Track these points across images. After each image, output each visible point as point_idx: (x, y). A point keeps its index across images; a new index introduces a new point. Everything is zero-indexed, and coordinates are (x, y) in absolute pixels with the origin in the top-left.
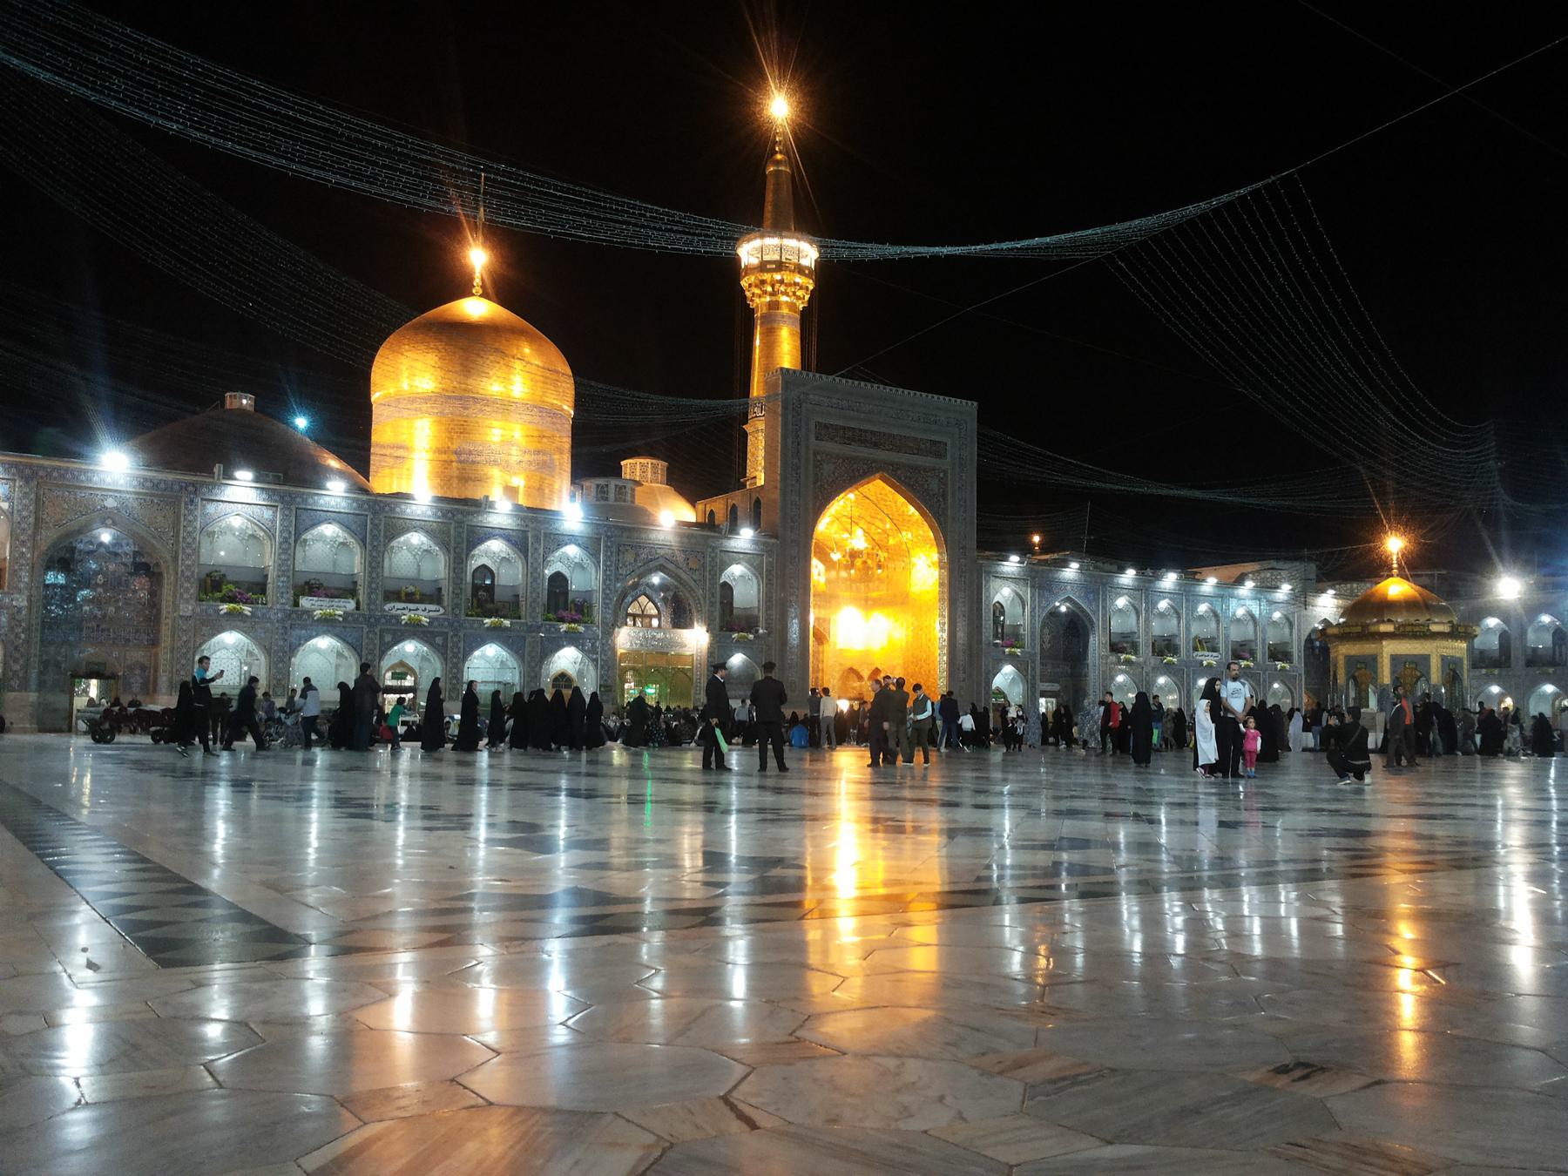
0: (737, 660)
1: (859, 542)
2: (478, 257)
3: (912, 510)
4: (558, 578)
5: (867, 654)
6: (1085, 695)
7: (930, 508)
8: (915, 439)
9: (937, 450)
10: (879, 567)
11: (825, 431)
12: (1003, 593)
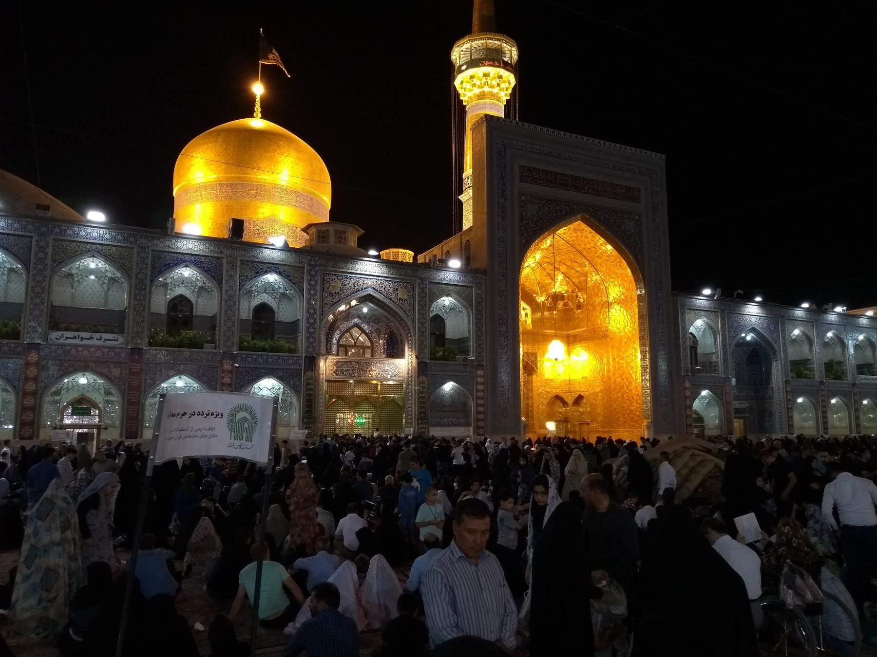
0: (448, 387)
1: (560, 286)
2: (258, 89)
3: (609, 247)
4: (263, 310)
5: (570, 382)
6: (771, 414)
7: (628, 246)
9: (631, 195)
10: (579, 307)
11: (530, 175)
12: (698, 325)
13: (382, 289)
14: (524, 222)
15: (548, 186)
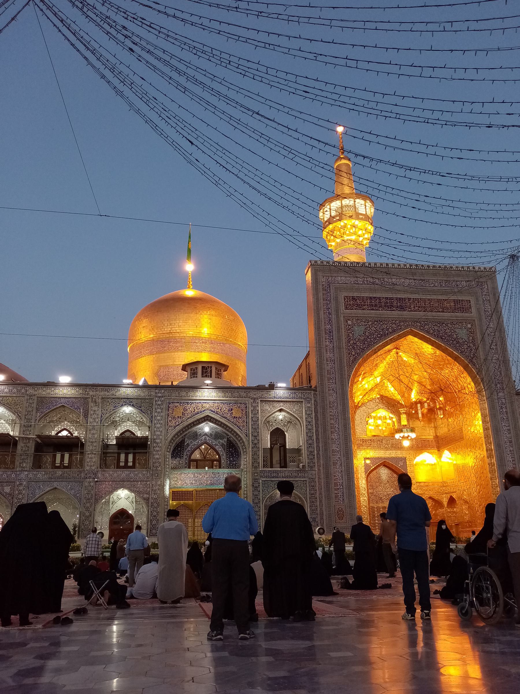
8: (439, 301)
13: (219, 410)
14: (352, 342)
15: (373, 310)
